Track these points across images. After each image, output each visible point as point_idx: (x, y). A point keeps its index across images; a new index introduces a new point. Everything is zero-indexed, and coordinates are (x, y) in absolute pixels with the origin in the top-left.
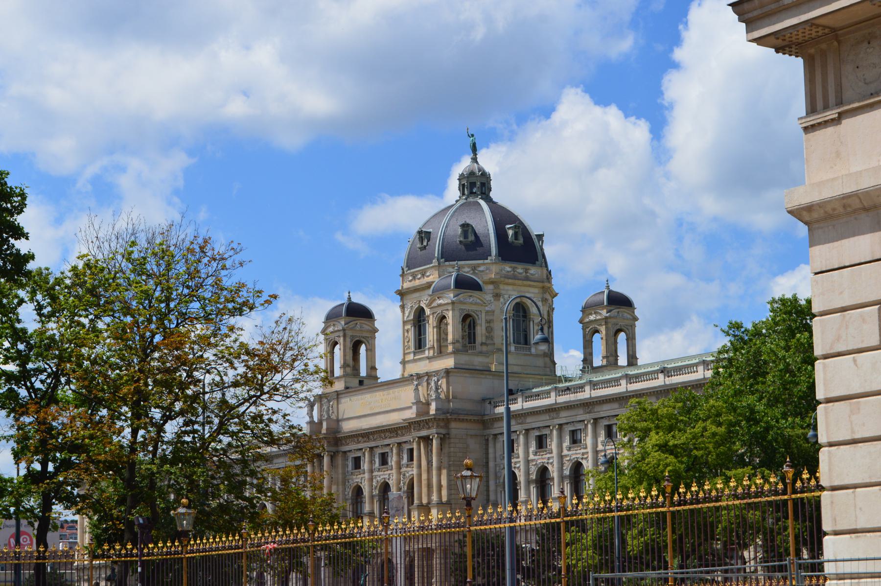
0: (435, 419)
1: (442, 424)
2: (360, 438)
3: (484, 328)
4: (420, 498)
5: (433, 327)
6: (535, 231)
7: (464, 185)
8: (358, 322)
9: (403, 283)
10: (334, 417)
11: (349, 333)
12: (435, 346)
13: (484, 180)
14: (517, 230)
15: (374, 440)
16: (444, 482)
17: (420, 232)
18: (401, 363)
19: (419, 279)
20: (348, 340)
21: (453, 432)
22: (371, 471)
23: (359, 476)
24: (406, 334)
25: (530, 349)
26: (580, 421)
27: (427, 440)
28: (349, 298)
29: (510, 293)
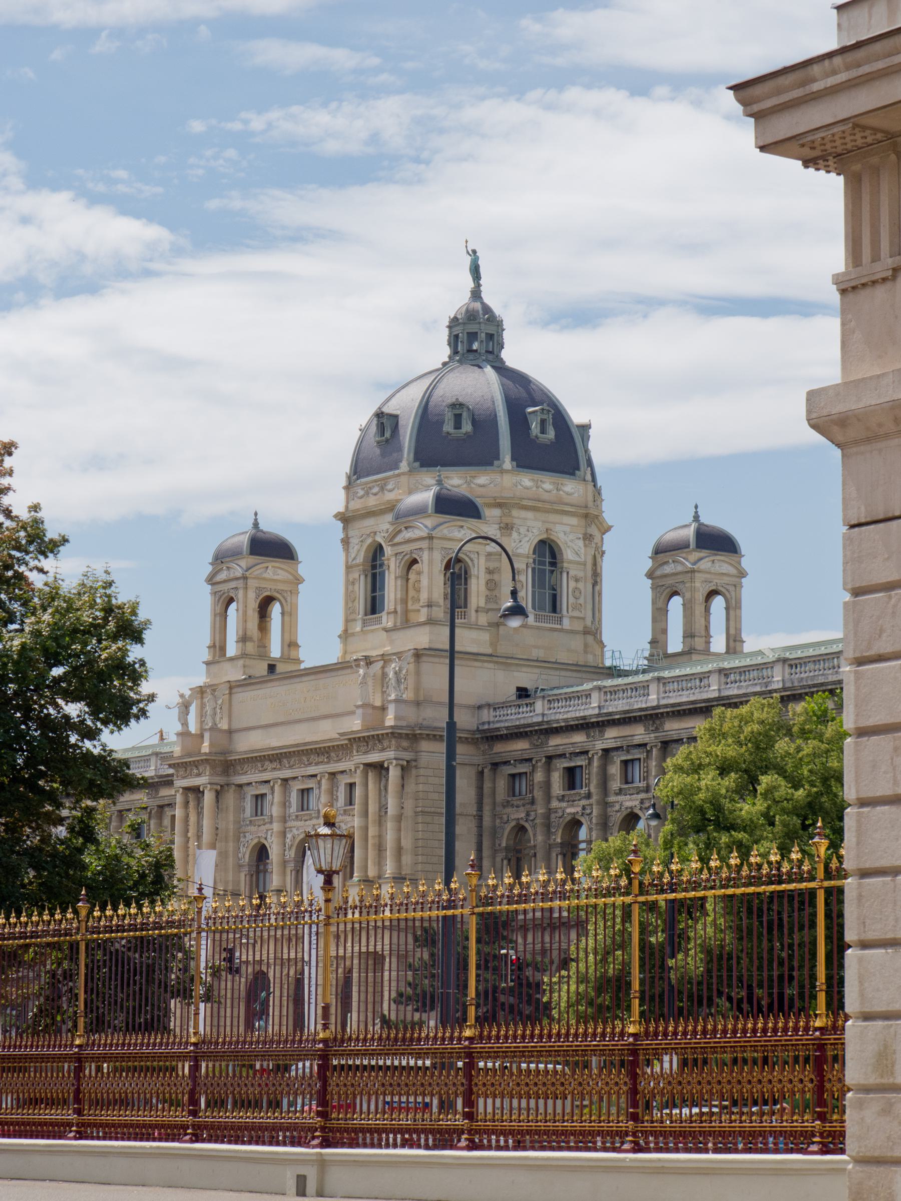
0: (395, 734)
1: (405, 744)
2: (267, 763)
3: (482, 582)
5: (396, 578)
6: (577, 416)
7: (457, 336)
8: (270, 565)
10: (224, 725)
11: (252, 583)
13: (491, 330)
14: (545, 417)
15: (291, 767)
16: (407, 843)
17: (379, 415)
18: (340, 636)
20: (251, 595)
21: (424, 759)
22: (284, 819)
23: (263, 827)
24: (350, 588)
25: (560, 621)
26: (640, 745)
28: (256, 525)
29: (529, 523)
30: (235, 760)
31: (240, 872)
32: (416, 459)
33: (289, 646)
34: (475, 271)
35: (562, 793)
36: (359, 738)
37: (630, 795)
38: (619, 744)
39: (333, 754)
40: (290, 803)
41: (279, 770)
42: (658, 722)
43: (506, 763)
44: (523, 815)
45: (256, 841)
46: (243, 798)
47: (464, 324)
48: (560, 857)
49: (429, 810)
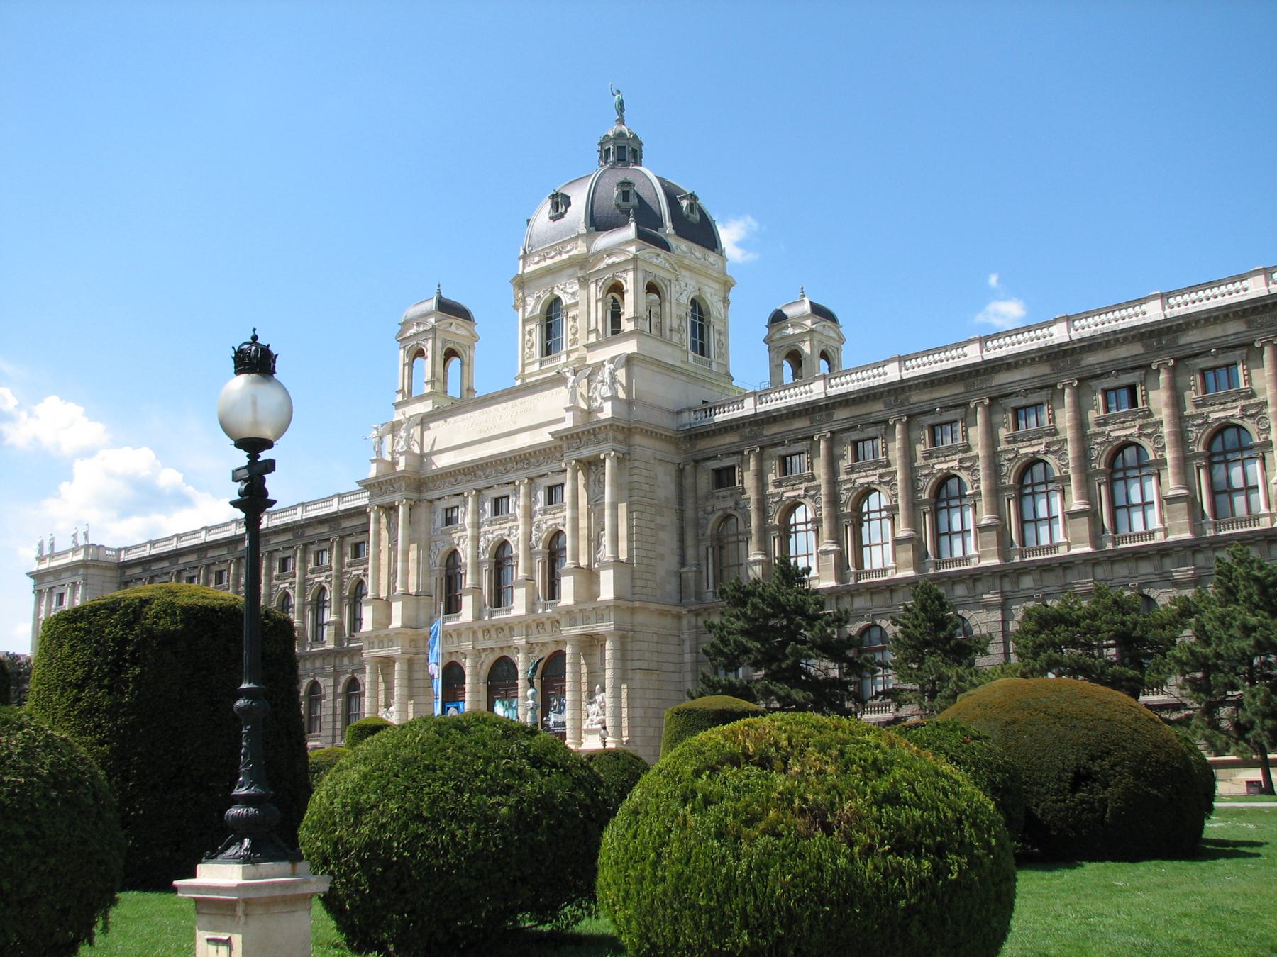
1: (620, 437)
4: (576, 556)
9: (524, 268)
10: (417, 450)
12: (600, 328)
14: (693, 202)
15: (486, 477)
19: (552, 258)
20: (439, 344)
22: (477, 525)
24: (527, 337)
27: (591, 466)
30: (428, 478)
31: (430, 576)
32: (591, 225)
33: (468, 390)
36: (572, 435)
37: (865, 471)
38: (852, 424)
39: (532, 460)
40: (484, 510)
42: (902, 397)
43: (709, 459)
44: (731, 504)
45: (447, 547)
46: (432, 512)
47: (615, 139)
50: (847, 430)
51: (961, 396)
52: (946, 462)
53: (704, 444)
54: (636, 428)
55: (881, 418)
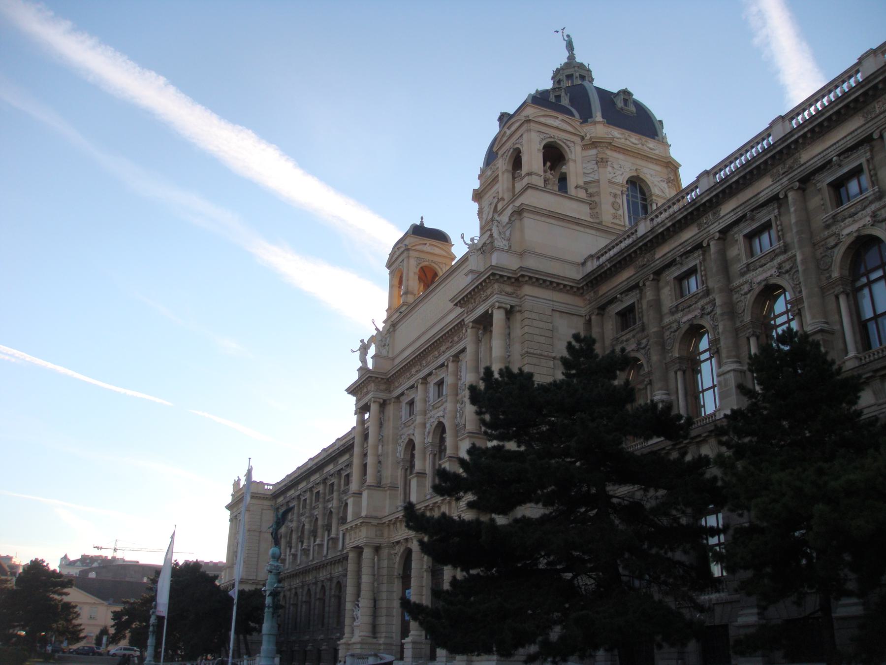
1: (509, 289)
34: (570, 46)
35: (675, 303)
37: (761, 266)
38: (740, 214)
41: (420, 371)
48: (679, 374)
49: (535, 352)
50: (736, 223)
51: (859, 131)
52: (855, 221)
53: (606, 289)
54: (523, 276)
55: (771, 194)
